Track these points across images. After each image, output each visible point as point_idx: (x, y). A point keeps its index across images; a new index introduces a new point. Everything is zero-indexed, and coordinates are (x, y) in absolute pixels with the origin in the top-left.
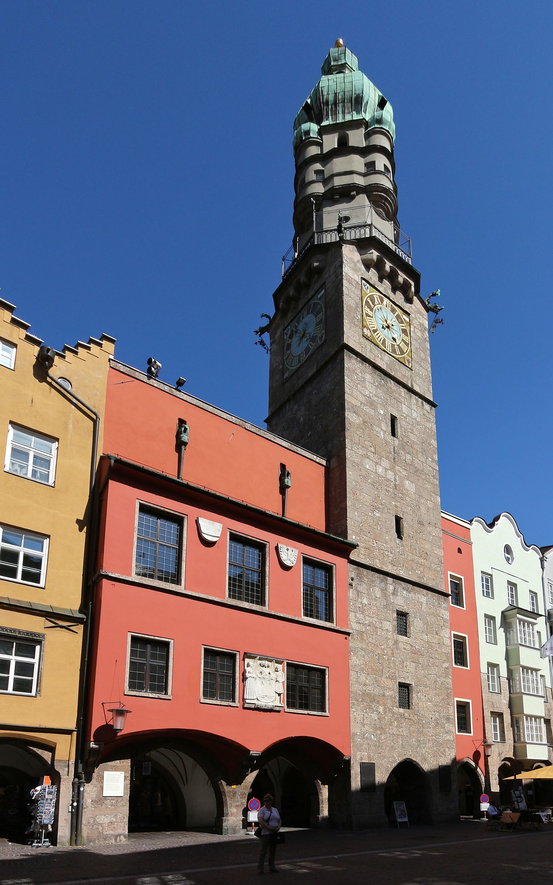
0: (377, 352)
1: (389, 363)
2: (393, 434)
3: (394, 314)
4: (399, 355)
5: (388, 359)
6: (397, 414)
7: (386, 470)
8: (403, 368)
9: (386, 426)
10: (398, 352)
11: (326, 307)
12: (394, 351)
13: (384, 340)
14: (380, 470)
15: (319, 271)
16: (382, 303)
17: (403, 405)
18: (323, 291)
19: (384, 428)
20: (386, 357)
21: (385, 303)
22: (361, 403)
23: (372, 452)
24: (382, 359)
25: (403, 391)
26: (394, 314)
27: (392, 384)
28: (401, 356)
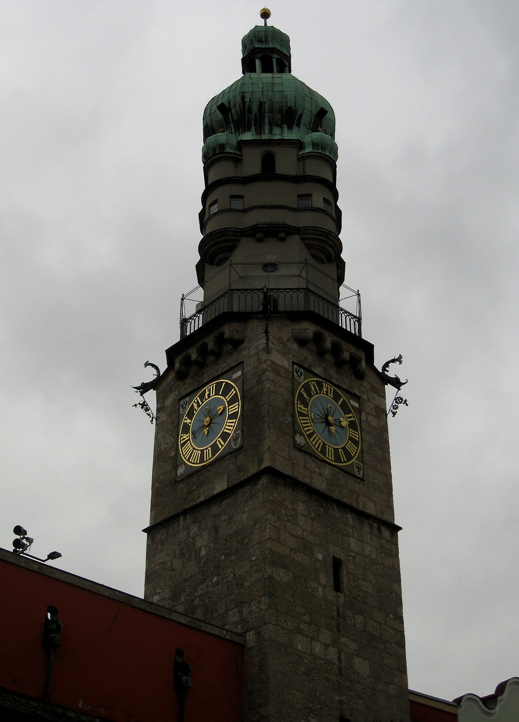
0: (313, 465)
2: (337, 587)
4: (345, 462)
6: (342, 555)
7: (327, 646)
9: (325, 578)
10: (343, 458)
11: (242, 398)
12: (337, 459)
13: (324, 445)
14: (318, 648)
16: (320, 391)
17: (352, 540)
18: (239, 373)
19: (323, 581)
20: (327, 471)
21: (325, 389)
22: (291, 549)
23: (306, 622)
24: (320, 474)
25: (350, 518)
27: (335, 512)
28: (345, 464)
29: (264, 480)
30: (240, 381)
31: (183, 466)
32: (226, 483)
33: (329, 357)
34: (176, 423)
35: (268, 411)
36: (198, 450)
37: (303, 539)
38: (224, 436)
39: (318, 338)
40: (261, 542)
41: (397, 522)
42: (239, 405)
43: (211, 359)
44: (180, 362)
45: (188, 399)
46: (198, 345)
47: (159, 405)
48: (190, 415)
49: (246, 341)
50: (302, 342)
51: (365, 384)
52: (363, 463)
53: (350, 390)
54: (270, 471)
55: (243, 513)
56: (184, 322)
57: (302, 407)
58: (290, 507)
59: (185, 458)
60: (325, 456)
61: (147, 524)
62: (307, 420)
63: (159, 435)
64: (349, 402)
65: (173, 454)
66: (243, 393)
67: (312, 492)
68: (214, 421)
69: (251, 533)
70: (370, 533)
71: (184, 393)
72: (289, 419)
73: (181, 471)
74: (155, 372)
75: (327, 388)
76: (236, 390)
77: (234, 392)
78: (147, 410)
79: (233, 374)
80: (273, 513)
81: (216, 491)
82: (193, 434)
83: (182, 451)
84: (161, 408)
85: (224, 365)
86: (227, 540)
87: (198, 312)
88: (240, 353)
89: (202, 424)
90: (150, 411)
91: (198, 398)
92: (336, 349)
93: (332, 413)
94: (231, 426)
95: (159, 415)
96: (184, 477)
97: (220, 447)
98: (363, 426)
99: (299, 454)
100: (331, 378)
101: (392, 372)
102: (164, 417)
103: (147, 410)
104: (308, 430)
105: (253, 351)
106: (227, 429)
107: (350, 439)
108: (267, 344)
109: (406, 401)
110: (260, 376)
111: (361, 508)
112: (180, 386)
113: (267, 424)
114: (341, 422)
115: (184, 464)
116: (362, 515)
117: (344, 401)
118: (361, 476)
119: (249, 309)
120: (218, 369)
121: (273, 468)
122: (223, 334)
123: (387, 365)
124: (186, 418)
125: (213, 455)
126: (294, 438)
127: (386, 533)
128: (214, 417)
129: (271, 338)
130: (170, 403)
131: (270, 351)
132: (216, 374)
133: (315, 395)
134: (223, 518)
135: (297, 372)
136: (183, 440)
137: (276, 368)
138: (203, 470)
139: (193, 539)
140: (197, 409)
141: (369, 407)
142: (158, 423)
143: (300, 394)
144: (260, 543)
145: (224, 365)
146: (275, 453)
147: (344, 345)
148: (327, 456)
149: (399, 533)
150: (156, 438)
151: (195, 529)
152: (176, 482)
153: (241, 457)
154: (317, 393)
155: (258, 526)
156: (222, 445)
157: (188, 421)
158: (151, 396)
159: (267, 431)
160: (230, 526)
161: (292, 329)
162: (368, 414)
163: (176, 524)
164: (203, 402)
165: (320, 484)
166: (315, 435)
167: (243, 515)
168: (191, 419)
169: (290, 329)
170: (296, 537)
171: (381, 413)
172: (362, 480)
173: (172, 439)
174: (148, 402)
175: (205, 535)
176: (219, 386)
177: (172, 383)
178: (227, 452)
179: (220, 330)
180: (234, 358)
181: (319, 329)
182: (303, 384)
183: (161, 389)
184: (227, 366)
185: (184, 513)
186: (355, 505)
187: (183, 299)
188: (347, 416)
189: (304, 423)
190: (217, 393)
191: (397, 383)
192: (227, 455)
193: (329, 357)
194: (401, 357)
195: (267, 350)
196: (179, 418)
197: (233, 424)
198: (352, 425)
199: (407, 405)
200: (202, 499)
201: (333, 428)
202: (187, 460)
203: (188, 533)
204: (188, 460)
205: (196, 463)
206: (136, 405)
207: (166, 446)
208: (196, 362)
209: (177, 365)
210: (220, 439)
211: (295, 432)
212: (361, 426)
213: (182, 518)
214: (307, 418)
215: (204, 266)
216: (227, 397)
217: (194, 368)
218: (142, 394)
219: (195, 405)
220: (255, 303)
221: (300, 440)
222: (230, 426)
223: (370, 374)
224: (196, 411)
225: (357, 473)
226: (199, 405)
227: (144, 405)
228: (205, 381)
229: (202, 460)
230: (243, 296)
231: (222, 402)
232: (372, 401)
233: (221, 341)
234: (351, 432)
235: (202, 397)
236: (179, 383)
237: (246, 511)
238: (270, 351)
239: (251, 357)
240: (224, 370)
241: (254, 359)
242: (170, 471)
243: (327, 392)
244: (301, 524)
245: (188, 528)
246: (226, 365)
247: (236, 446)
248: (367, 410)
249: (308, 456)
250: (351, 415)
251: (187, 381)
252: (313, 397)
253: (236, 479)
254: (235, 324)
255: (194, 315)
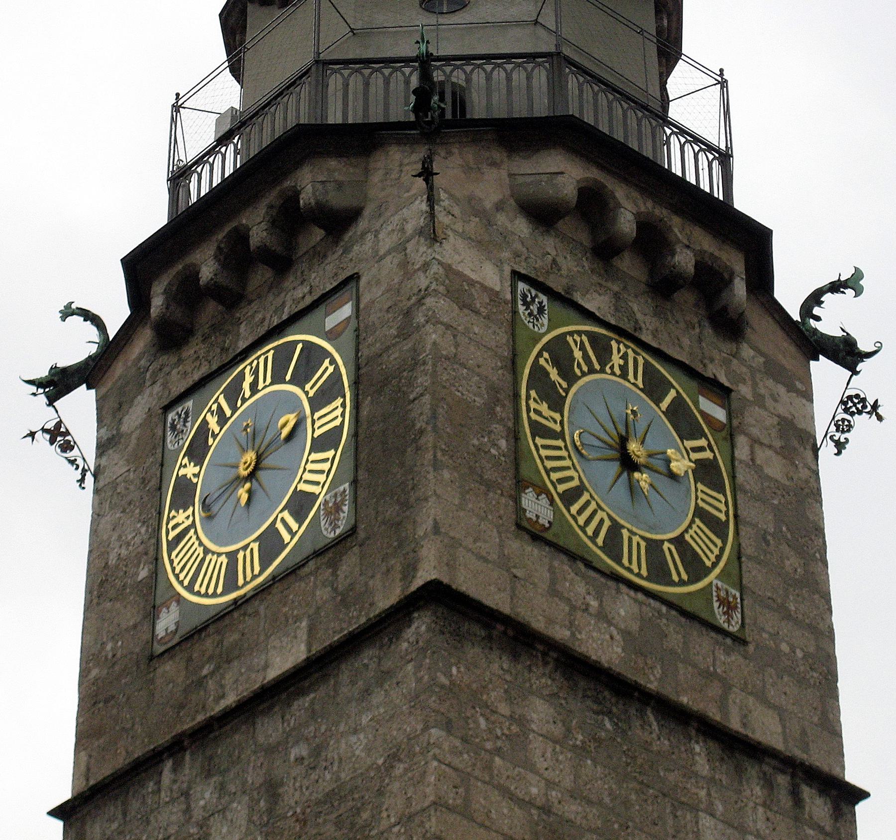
1: (635, 627)
3: (658, 402)
4: (682, 583)
5: (636, 609)
8: (703, 646)
10: (677, 569)
11: (356, 383)
12: (659, 571)
13: (615, 528)
15: (338, 222)
17: (706, 821)
18: (346, 311)
20: (625, 608)
24: (602, 616)
26: (658, 402)
29: (421, 625)
30: (348, 336)
31: (174, 607)
32: (303, 647)
33: (627, 263)
34: (154, 482)
35: (434, 416)
36: (219, 555)
37: (546, 810)
38: (300, 504)
39: (592, 205)
40: (411, 817)
41: (853, 776)
42: (343, 405)
43: (261, 275)
44: (165, 292)
45: (189, 404)
46: (220, 236)
47: (103, 430)
48: (197, 452)
49: (366, 213)
50: (543, 214)
51: (747, 352)
52: (741, 588)
53: (699, 368)
54: (439, 596)
55: (355, 732)
56: (179, 177)
57: (544, 407)
58: (504, 709)
59: (181, 583)
60: (618, 560)
61: (64, 793)
62: (559, 448)
63: (103, 521)
64: (696, 403)
65: (143, 573)
66: (358, 368)
67: (574, 666)
68: (266, 462)
69: (380, 793)
70: (764, 805)
71: (179, 387)
72: (503, 443)
73: (167, 622)
74: (93, 333)
75: (625, 357)
76: (336, 362)
77: (331, 369)
78: (67, 447)
79: (327, 314)
80: (448, 727)
81: (272, 674)
82: (205, 506)
83: (171, 562)
84: (110, 440)
85: (299, 293)
86: (305, 822)
87: (223, 140)
88: (346, 250)
89: (232, 474)
90: (75, 453)
91: (222, 401)
92: (651, 241)
93: (640, 434)
94: (321, 472)
95: (104, 461)
96: (176, 639)
97: (286, 537)
98: (740, 478)
99: (533, 551)
100: (637, 328)
101: (831, 320)
102: (118, 466)
103: (67, 447)
104: (561, 481)
105: (387, 241)
106: (306, 482)
107: (700, 513)
108: (432, 215)
109: (875, 406)
110: (408, 313)
111: (735, 724)
112: (166, 369)
113: (429, 456)
114: (668, 461)
115: (178, 602)
116: (737, 747)
117: (678, 399)
118: (734, 628)
119: (376, 116)
120: (284, 302)
121: (448, 587)
122: (295, 195)
123: (815, 298)
124: (186, 460)
125: (265, 563)
126: (517, 500)
127: (818, 807)
128: (266, 452)
129: (443, 195)
130: (140, 421)
131: (439, 240)
132: (276, 321)
133: (584, 374)
134: (294, 753)
135: (527, 304)
136: (174, 528)
137: (458, 289)
138: (236, 615)
139: (203, 824)
140: (217, 430)
141: (759, 421)
142: (101, 484)
143: (538, 373)
144: (406, 819)
145: (299, 293)
146: (454, 538)
147: (678, 228)
148: (625, 561)
149: (861, 808)
150: (94, 532)
151: (207, 795)
152: (152, 658)
153: (349, 564)
154: (592, 371)
155: (400, 768)
156: (292, 533)
157: (190, 470)
158: (80, 408)
159: (430, 476)
160: (314, 776)
161: (510, 175)
162: (755, 441)
163: (151, 786)
164: (234, 409)
165: (603, 646)
166: (585, 497)
167: (353, 739)
168: (199, 462)
169: (504, 174)
170: (526, 804)
171: (799, 442)
172: (739, 640)
173: (143, 530)
174: (69, 423)
175: (239, 810)
176: (282, 357)
177: (143, 362)
178: (308, 550)
179: (287, 184)
180: (329, 268)
181: (594, 174)
182: (545, 340)
183: (109, 384)
184: (310, 292)
185: (175, 748)
186: (714, 714)
187: (176, 108)
188: (690, 444)
189: (549, 458)
190: (278, 378)
191: (847, 353)
192: (307, 560)
193: (627, 263)
194: (858, 275)
195: (432, 234)
196: (163, 465)
197: (326, 466)
198: (706, 472)
199: (880, 418)
200: (231, 699)
201: (643, 478)
202: (186, 588)
203: (188, 810)
204: (190, 588)
205: (215, 595)
206: (32, 435)
207: (124, 552)
208: (216, 291)
209: (157, 303)
210: (286, 515)
211: (520, 484)
212: (733, 477)
213: (169, 764)
214: (560, 443)
215: (244, 13)
216: (308, 387)
217: (211, 309)
218: (52, 400)
219: (213, 421)
220: (393, 99)
221: (535, 507)
222: (317, 473)
223: (760, 325)
224: (215, 436)
225: (721, 620)
226: (222, 420)
227: (57, 434)
228: (242, 345)
229: (231, 583)
230: (356, 82)
231: (292, 403)
232: (769, 403)
233: (291, 218)
234: (701, 494)
235: (233, 394)
236: (163, 359)
237: (364, 726)
238: (439, 240)
239: (382, 258)
240: (302, 306)
241: (390, 263)
242: (135, 626)
243: (624, 369)
244: (541, 765)
245: (186, 794)
246: (306, 290)
247: (334, 529)
248: (755, 431)
249: (563, 557)
250: (702, 442)
251: (188, 352)
252: (581, 382)
253: (333, 632)
254: (333, 163)
255: (211, 151)
